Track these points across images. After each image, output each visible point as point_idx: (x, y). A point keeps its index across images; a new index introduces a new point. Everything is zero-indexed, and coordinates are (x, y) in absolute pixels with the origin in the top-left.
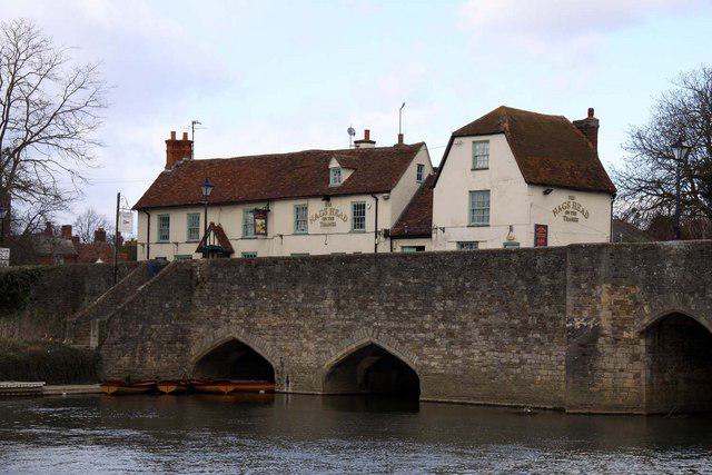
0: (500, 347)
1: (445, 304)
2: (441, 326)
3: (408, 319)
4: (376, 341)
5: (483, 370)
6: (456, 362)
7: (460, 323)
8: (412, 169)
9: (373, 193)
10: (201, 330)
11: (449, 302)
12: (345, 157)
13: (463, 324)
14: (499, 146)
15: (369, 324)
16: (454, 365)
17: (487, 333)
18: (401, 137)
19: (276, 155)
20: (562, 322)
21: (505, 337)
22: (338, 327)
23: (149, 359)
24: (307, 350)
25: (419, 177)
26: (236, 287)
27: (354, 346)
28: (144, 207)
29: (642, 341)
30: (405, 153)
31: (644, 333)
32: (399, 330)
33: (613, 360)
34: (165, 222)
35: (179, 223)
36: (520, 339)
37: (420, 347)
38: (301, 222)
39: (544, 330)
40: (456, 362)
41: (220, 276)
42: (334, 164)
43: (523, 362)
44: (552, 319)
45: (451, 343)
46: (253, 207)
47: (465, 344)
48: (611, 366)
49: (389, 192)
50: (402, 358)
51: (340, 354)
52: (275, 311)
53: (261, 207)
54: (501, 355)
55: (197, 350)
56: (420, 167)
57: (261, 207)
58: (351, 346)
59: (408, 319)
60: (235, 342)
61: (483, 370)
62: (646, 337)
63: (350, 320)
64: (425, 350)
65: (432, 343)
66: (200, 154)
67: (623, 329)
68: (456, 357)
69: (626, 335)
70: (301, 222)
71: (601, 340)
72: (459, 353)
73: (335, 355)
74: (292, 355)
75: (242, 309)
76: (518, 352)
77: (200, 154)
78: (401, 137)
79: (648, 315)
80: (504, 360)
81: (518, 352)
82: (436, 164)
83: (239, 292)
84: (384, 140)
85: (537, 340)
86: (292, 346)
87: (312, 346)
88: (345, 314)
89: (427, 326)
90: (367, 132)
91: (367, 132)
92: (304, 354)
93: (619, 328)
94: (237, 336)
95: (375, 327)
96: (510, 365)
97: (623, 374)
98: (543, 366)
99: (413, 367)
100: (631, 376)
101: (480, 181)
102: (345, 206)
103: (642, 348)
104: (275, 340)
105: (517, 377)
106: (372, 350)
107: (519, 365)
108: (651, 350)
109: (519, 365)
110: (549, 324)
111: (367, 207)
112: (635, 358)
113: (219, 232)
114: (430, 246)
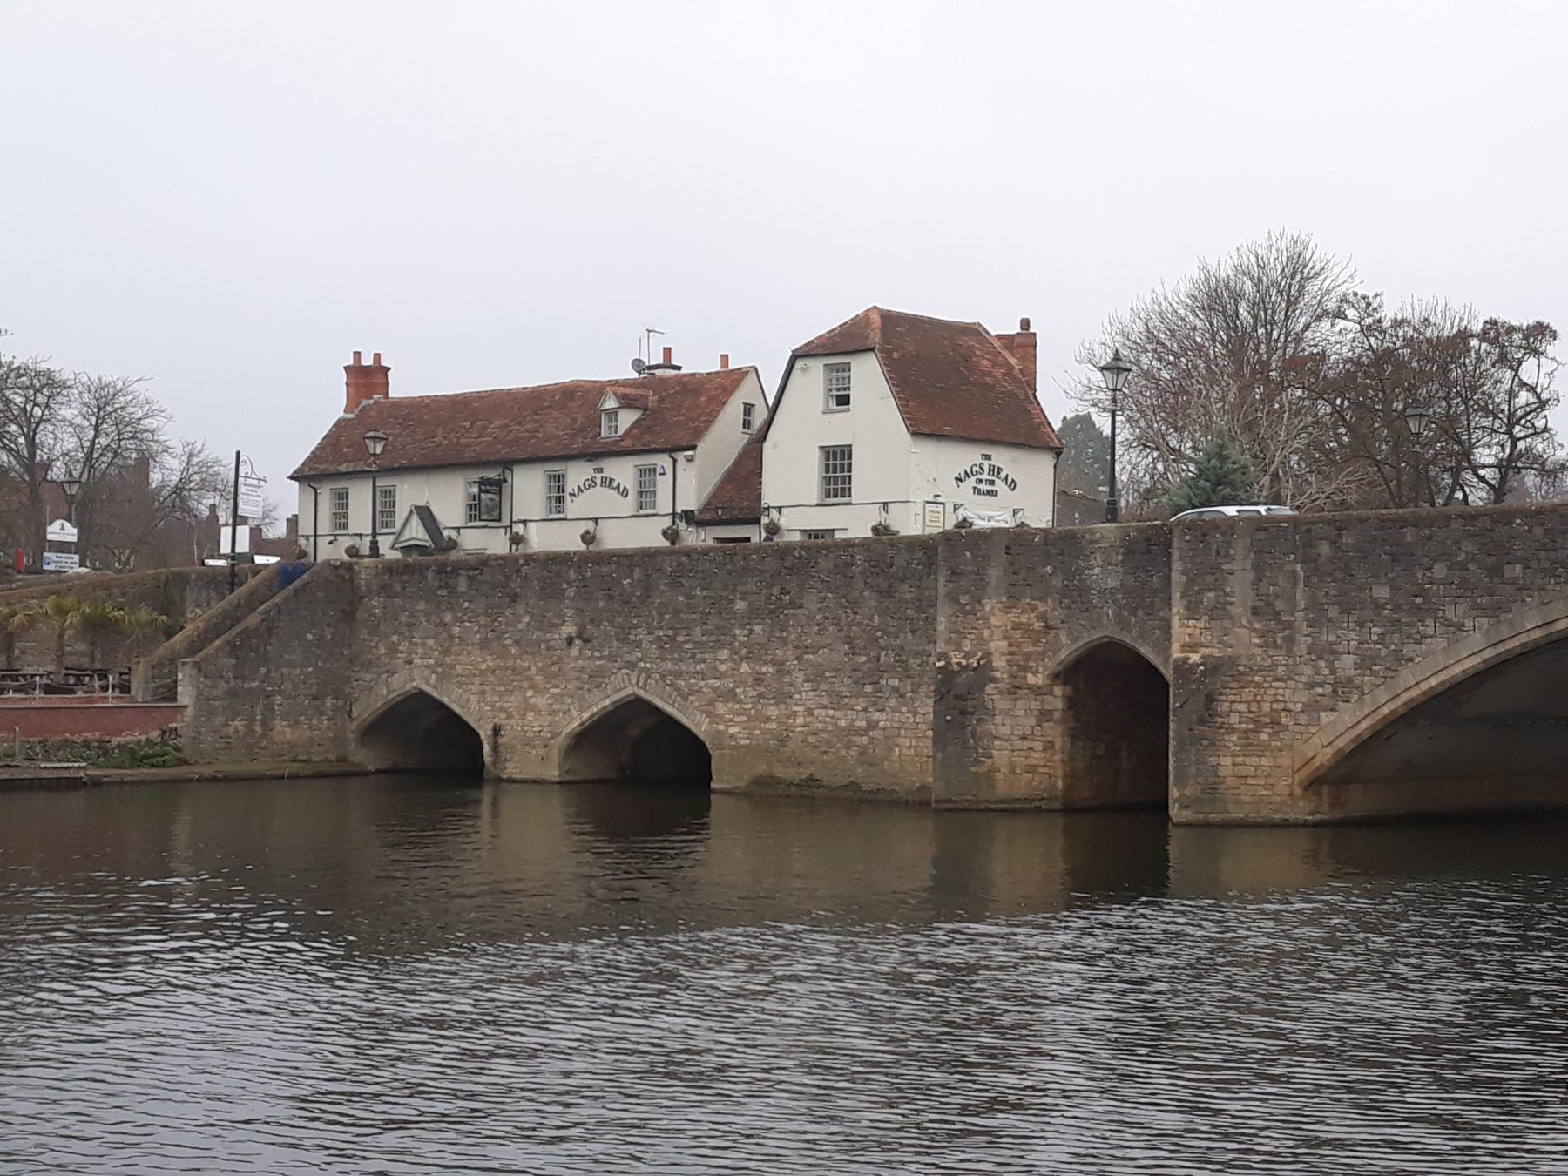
0: (838, 702)
1: (751, 631)
2: (745, 667)
3: (693, 657)
4: (641, 693)
5: (812, 739)
6: (767, 726)
7: (774, 663)
8: (732, 412)
9: (672, 450)
10: (368, 677)
11: (758, 629)
12: (629, 396)
13: (780, 665)
14: (868, 375)
15: (631, 665)
16: (765, 731)
17: (816, 677)
18: (725, 358)
19: (491, 394)
20: (932, 659)
21: (844, 685)
22: (582, 670)
23: (279, 725)
24: (534, 708)
25: (747, 424)
26: (421, 606)
27: (607, 702)
28: (306, 476)
29: (1058, 691)
30: (730, 380)
31: (1055, 677)
32: (679, 674)
33: (1008, 721)
34: (342, 498)
35: (361, 499)
36: (868, 688)
37: (711, 703)
38: (557, 496)
39: (906, 674)
40: (767, 726)
41: (398, 587)
42: (610, 403)
43: (872, 725)
44: (917, 654)
45: (761, 696)
46: (477, 475)
47: (782, 697)
48: (1005, 731)
49: (694, 448)
50: (685, 721)
51: (586, 715)
52: (484, 645)
53: (492, 474)
54: (838, 714)
55: (367, 707)
56: (748, 408)
57: (492, 474)
58: (601, 703)
59: (693, 657)
60: (421, 694)
61: (812, 739)
62: (1065, 684)
63: (600, 658)
64: (721, 708)
65: (729, 696)
66: (401, 387)
67: (1026, 669)
68: (768, 719)
69: (1031, 679)
70: (557, 496)
71: (990, 689)
72: (772, 711)
73: (576, 719)
74: (510, 716)
75: (431, 642)
76: (865, 710)
77: (401, 387)
78: (725, 358)
79: (1067, 648)
80: (843, 723)
81: (865, 710)
82: (770, 403)
83: (428, 614)
84: (696, 361)
85: (895, 690)
86: (513, 701)
87: (542, 702)
88: (593, 649)
89: (723, 667)
90: (667, 351)
91: (667, 351)
92: (530, 716)
93: (1020, 667)
94: (425, 688)
95: (642, 670)
96: (851, 730)
97: (1026, 744)
98: (903, 732)
99: (702, 736)
100: (1038, 745)
101: (837, 430)
102: (624, 471)
103: (1056, 701)
104: (483, 693)
105: (863, 751)
106: (636, 708)
107: (867, 731)
108: (1072, 703)
109: (867, 731)
110: (913, 663)
111: (659, 470)
112: (1045, 716)
113: (425, 515)
114: (755, 535)
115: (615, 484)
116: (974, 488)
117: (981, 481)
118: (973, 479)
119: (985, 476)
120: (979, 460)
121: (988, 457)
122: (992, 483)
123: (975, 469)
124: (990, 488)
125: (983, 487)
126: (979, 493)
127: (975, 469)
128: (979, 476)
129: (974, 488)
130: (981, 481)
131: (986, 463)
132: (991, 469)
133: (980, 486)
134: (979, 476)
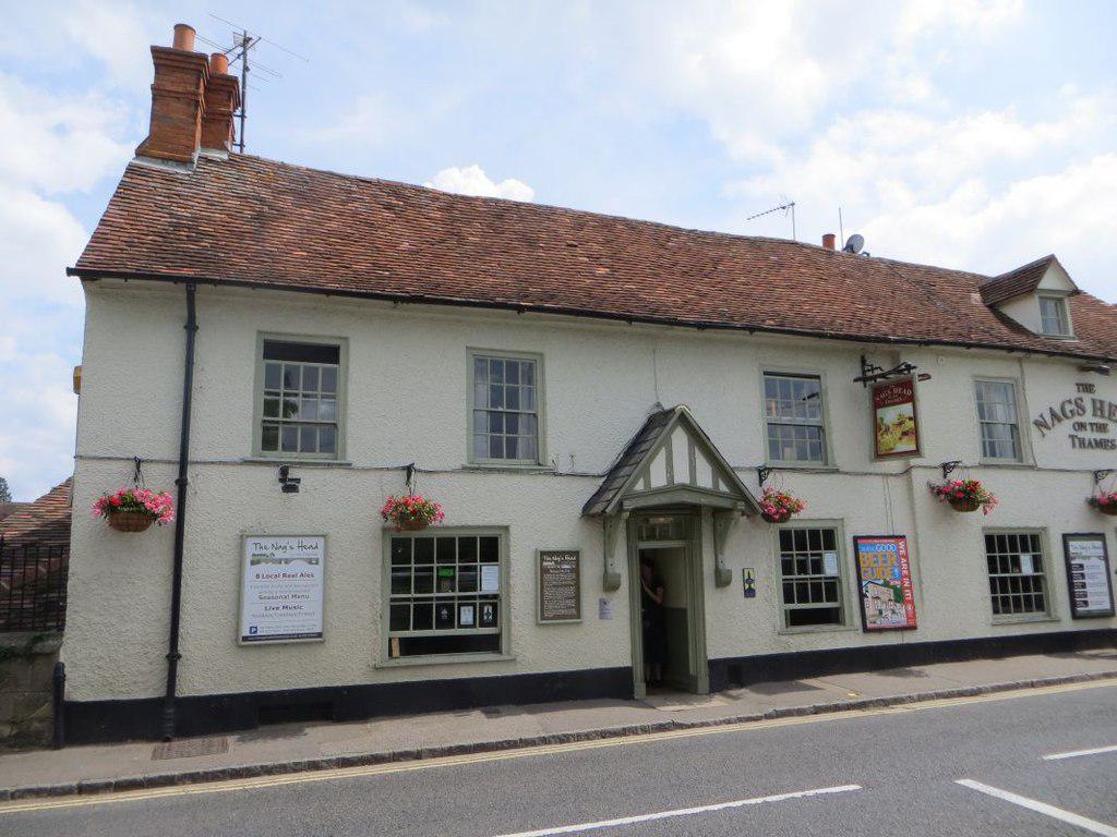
115: (1048, 418)
116: (1072, 437)
117: (1082, 426)
118: (1071, 422)
119: (1088, 418)
120: (1071, 392)
121: (1088, 388)
122: (1102, 428)
123: (1068, 408)
124: (1099, 436)
125: (1088, 435)
126: (1082, 443)
127: (1068, 408)
128: (1078, 419)
129: (1072, 437)
130: (1082, 426)
131: (1087, 399)
132: (1099, 407)
133: (1081, 434)
134: (1078, 419)
